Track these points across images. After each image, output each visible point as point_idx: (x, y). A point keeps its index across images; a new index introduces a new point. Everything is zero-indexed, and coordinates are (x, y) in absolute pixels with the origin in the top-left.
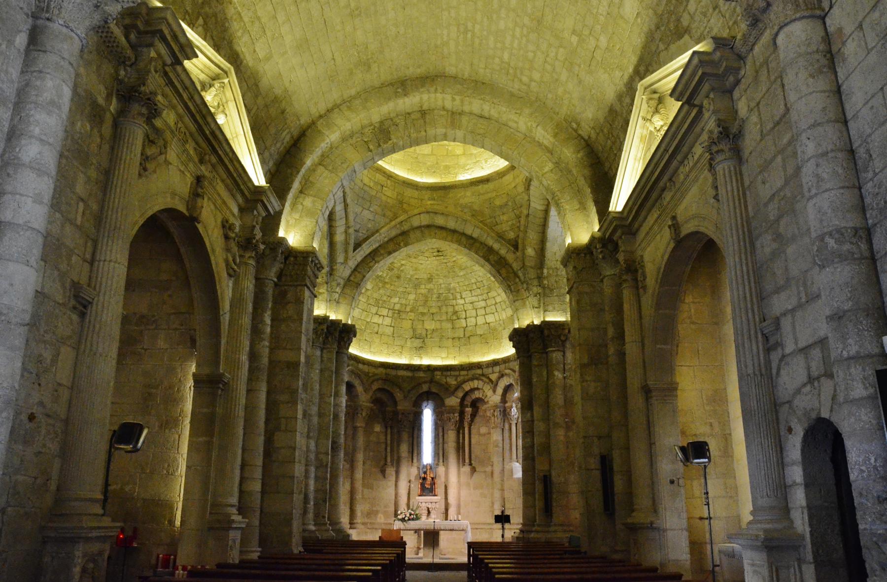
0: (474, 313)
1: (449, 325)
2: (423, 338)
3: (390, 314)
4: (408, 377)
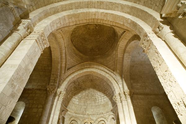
0: (100, 98)
1: (94, 102)
3: (78, 99)
4: (82, 117)
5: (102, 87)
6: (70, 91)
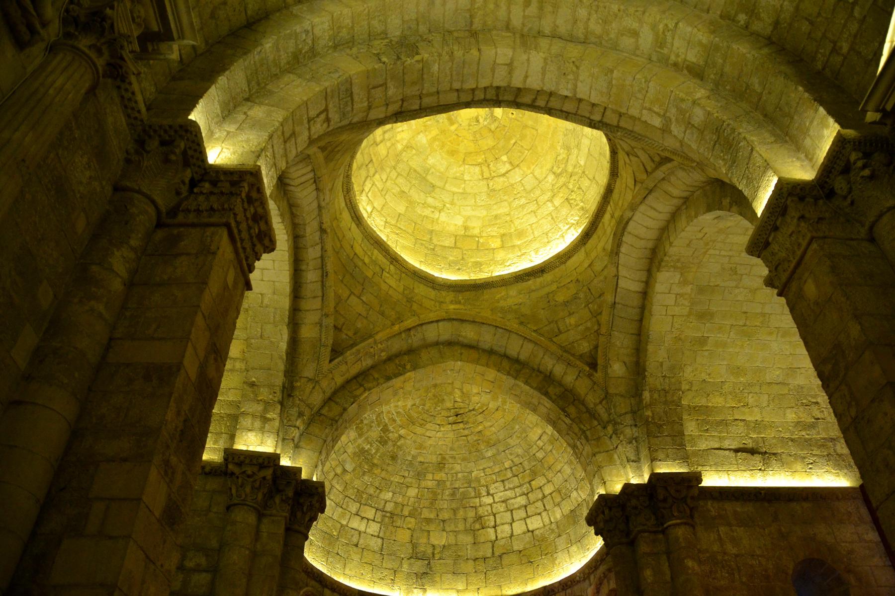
0: (507, 517)
1: (469, 539)
2: (428, 559)
5: (520, 451)
6: (336, 475)
